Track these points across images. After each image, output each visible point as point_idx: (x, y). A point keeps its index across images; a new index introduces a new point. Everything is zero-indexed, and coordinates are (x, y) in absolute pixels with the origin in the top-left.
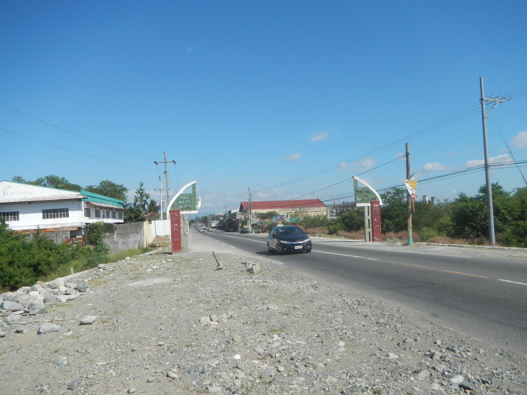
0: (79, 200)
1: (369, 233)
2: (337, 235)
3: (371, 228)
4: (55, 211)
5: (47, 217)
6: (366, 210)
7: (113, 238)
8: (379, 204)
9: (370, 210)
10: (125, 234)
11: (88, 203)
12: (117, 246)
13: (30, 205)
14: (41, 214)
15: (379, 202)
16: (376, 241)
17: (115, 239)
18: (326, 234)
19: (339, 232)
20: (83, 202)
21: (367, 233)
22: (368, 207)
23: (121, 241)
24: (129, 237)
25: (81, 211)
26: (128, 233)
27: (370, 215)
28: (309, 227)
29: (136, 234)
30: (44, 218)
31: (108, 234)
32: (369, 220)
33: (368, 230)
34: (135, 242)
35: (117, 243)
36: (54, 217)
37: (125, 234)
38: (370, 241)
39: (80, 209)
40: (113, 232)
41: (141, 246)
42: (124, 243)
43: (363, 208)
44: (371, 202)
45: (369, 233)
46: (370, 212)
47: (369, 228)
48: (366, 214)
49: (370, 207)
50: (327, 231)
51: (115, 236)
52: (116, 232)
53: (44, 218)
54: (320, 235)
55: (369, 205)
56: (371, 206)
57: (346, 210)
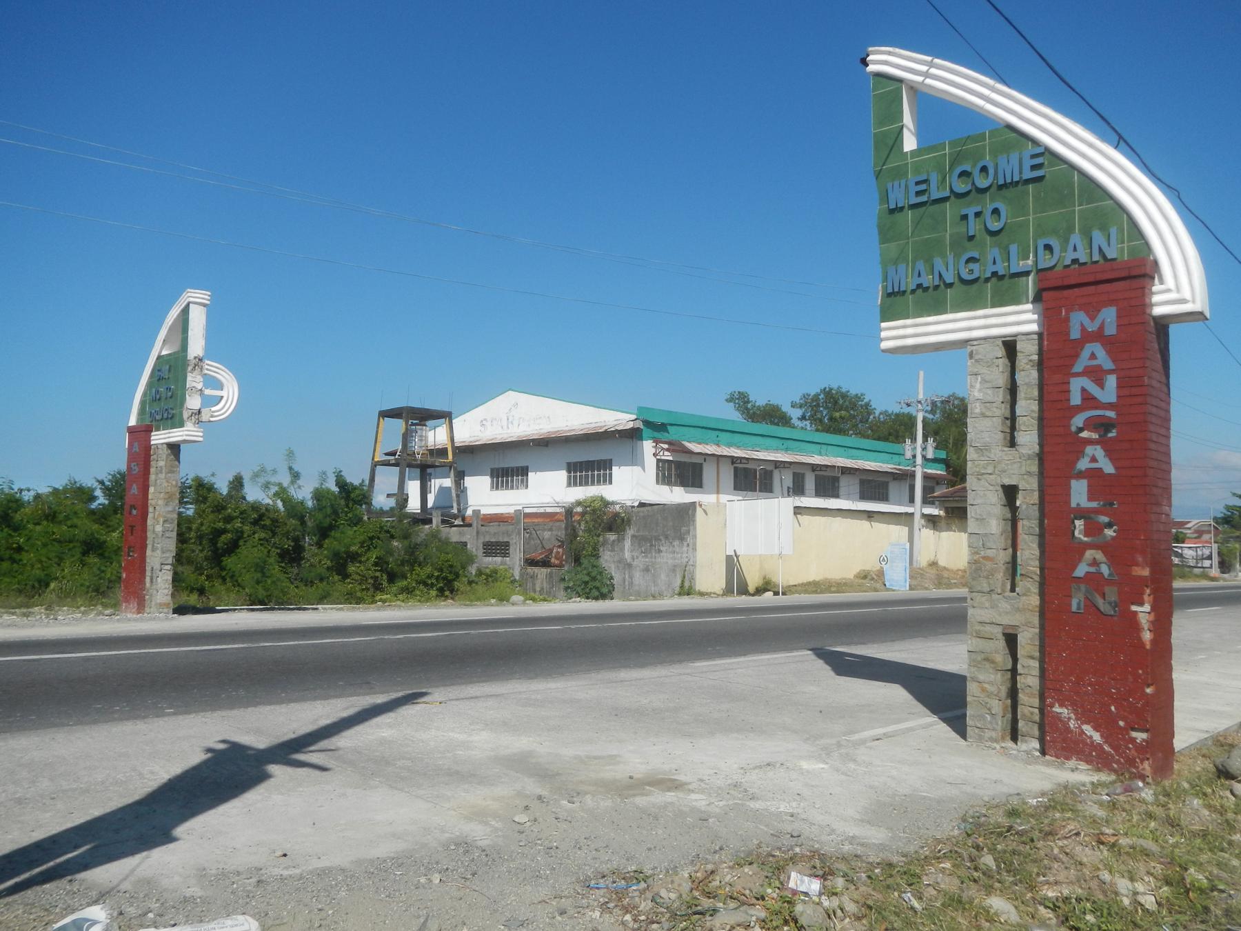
0: (632, 435)
4: (589, 466)
5: (575, 485)
7: (622, 550)
10: (650, 541)
11: (675, 447)
12: (631, 577)
13: (545, 447)
14: (562, 475)
17: (627, 555)
20: (648, 446)
23: (640, 562)
24: (660, 551)
25: (637, 469)
26: (657, 539)
27: (1029, 438)
29: (676, 543)
30: (569, 485)
31: (612, 537)
34: (673, 569)
35: (630, 566)
36: (587, 484)
37: (650, 541)
39: (635, 459)
40: (624, 530)
41: (687, 584)
42: (647, 570)
46: (1028, 406)
51: (627, 543)
52: (630, 532)
53: (569, 485)
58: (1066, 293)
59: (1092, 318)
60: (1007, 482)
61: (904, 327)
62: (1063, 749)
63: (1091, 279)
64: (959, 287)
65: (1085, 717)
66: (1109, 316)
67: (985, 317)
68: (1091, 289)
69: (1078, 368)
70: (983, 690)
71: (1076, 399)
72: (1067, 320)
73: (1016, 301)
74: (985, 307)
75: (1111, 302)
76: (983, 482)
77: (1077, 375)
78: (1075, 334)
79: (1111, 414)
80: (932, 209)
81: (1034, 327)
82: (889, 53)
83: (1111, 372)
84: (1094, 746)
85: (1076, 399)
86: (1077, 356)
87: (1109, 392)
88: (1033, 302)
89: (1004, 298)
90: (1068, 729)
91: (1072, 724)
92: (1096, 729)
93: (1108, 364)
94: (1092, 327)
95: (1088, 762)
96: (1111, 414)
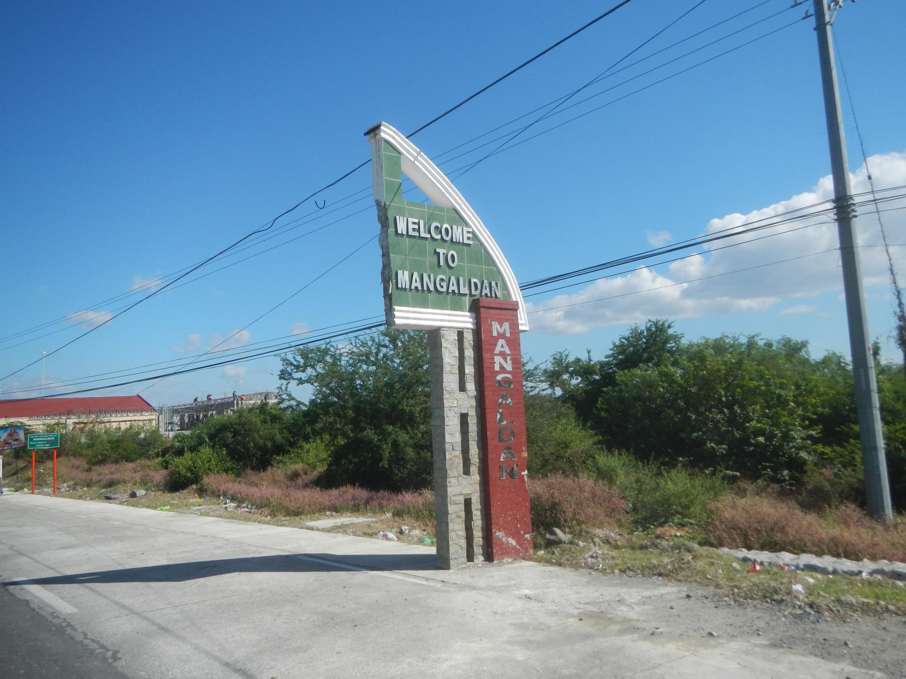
1: (468, 503)
2: (202, 492)
3: (476, 477)
6: (449, 357)
8: (514, 325)
9: (469, 353)
15: (514, 308)
16: (507, 551)
18: (158, 488)
19: (208, 480)
21: (455, 510)
22: (460, 334)
27: (471, 386)
28: (102, 461)
32: (464, 417)
33: (461, 486)
38: (470, 557)
43: (433, 336)
44: (475, 307)
45: (468, 503)
46: (470, 370)
47: (467, 472)
48: (450, 380)
49: (469, 337)
50: (160, 475)
54: (133, 495)
55: (464, 320)
56: (477, 332)
57: (205, 416)
58: (490, 311)
59: (501, 327)
60: (464, 411)
61: (408, 312)
62: (502, 554)
63: (499, 306)
64: (434, 294)
65: (508, 534)
66: (506, 325)
67: (449, 315)
68: (498, 311)
69: (496, 352)
70: (458, 535)
71: (497, 368)
72: (491, 326)
73: (461, 309)
74: (447, 309)
75: (507, 320)
76: (452, 412)
77: (497, 355)
78: (495, 334)
79: (510, 376)
80: (420, 241)
81: (471, 326)
82: (395, 132)
83: (509, 355)
84: (514, 548)
85: (497, 368)
86: (496, 345)
87: (509, 367)
88: (469, 311)
89: (456, 307)
90: (503, 543)
91: (504, 540)
92: (513, 538)
93: (508, 352)
94: (501, 331)
95: (511, 557)
96: (510, 376)
